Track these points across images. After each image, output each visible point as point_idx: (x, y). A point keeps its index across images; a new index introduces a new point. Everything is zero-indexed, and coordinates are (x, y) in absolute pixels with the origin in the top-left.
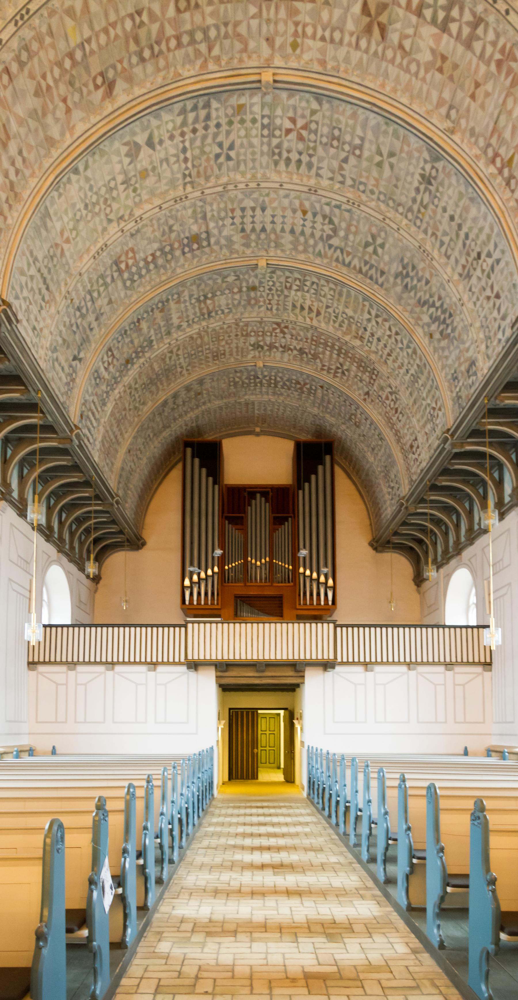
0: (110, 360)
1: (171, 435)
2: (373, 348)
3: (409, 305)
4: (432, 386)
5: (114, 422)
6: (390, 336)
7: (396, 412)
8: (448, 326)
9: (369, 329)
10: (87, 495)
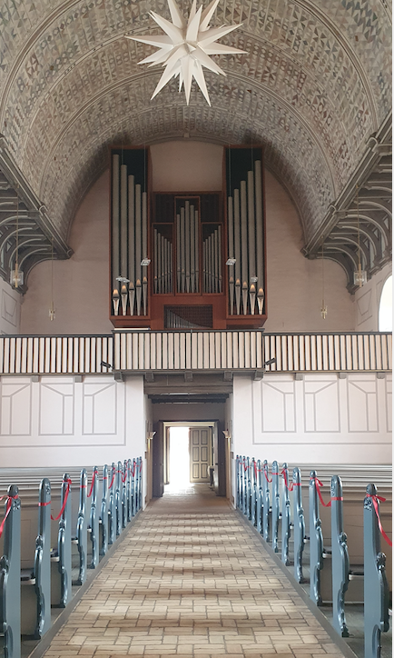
0: (34, 66)
1: (97, 142)
2: (300, 52)
3: (334, 7)
4: (358, 90)
6: (316, 39)
8: (372, 27)
9: (295, 32)
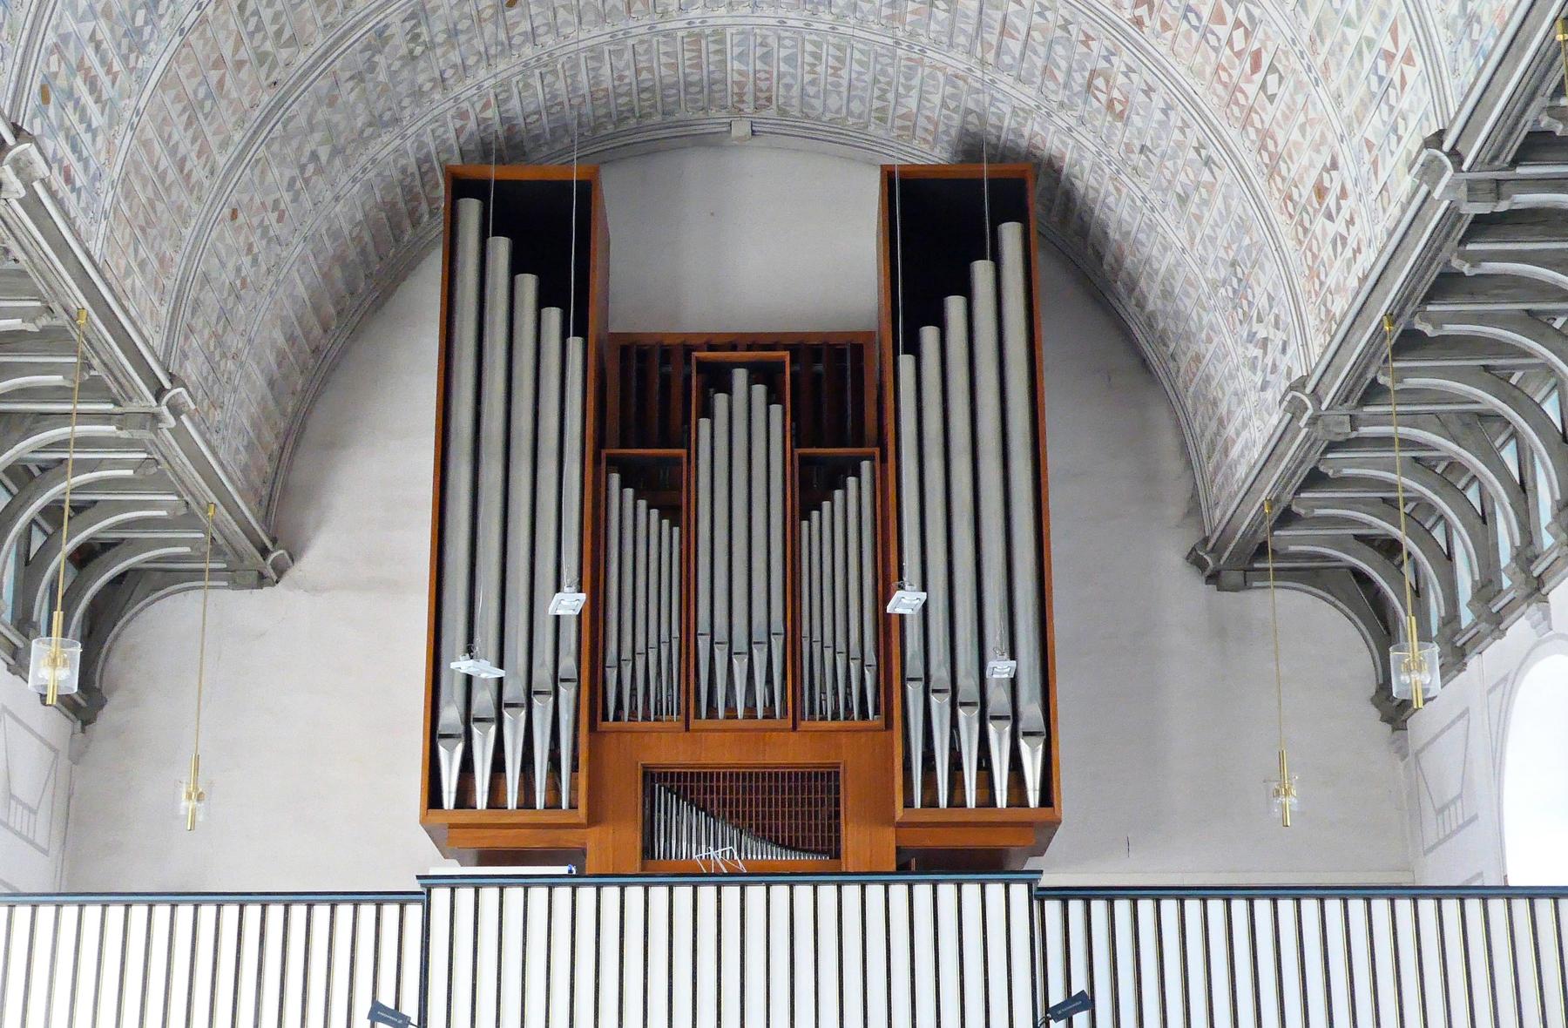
1: (399, 152)
5: (175, 109)
7: (1256, 66)
10: (56, 379)
